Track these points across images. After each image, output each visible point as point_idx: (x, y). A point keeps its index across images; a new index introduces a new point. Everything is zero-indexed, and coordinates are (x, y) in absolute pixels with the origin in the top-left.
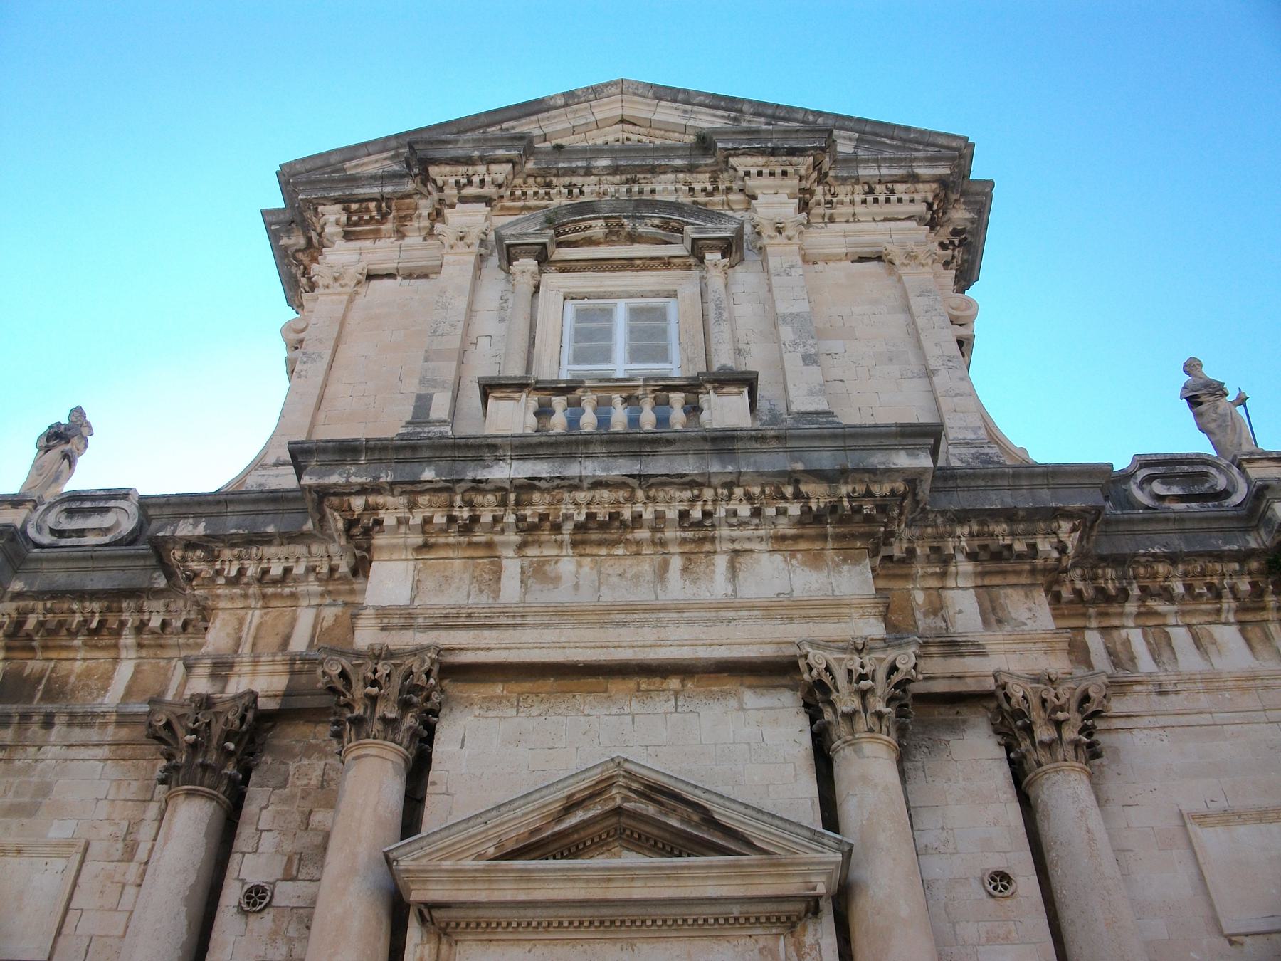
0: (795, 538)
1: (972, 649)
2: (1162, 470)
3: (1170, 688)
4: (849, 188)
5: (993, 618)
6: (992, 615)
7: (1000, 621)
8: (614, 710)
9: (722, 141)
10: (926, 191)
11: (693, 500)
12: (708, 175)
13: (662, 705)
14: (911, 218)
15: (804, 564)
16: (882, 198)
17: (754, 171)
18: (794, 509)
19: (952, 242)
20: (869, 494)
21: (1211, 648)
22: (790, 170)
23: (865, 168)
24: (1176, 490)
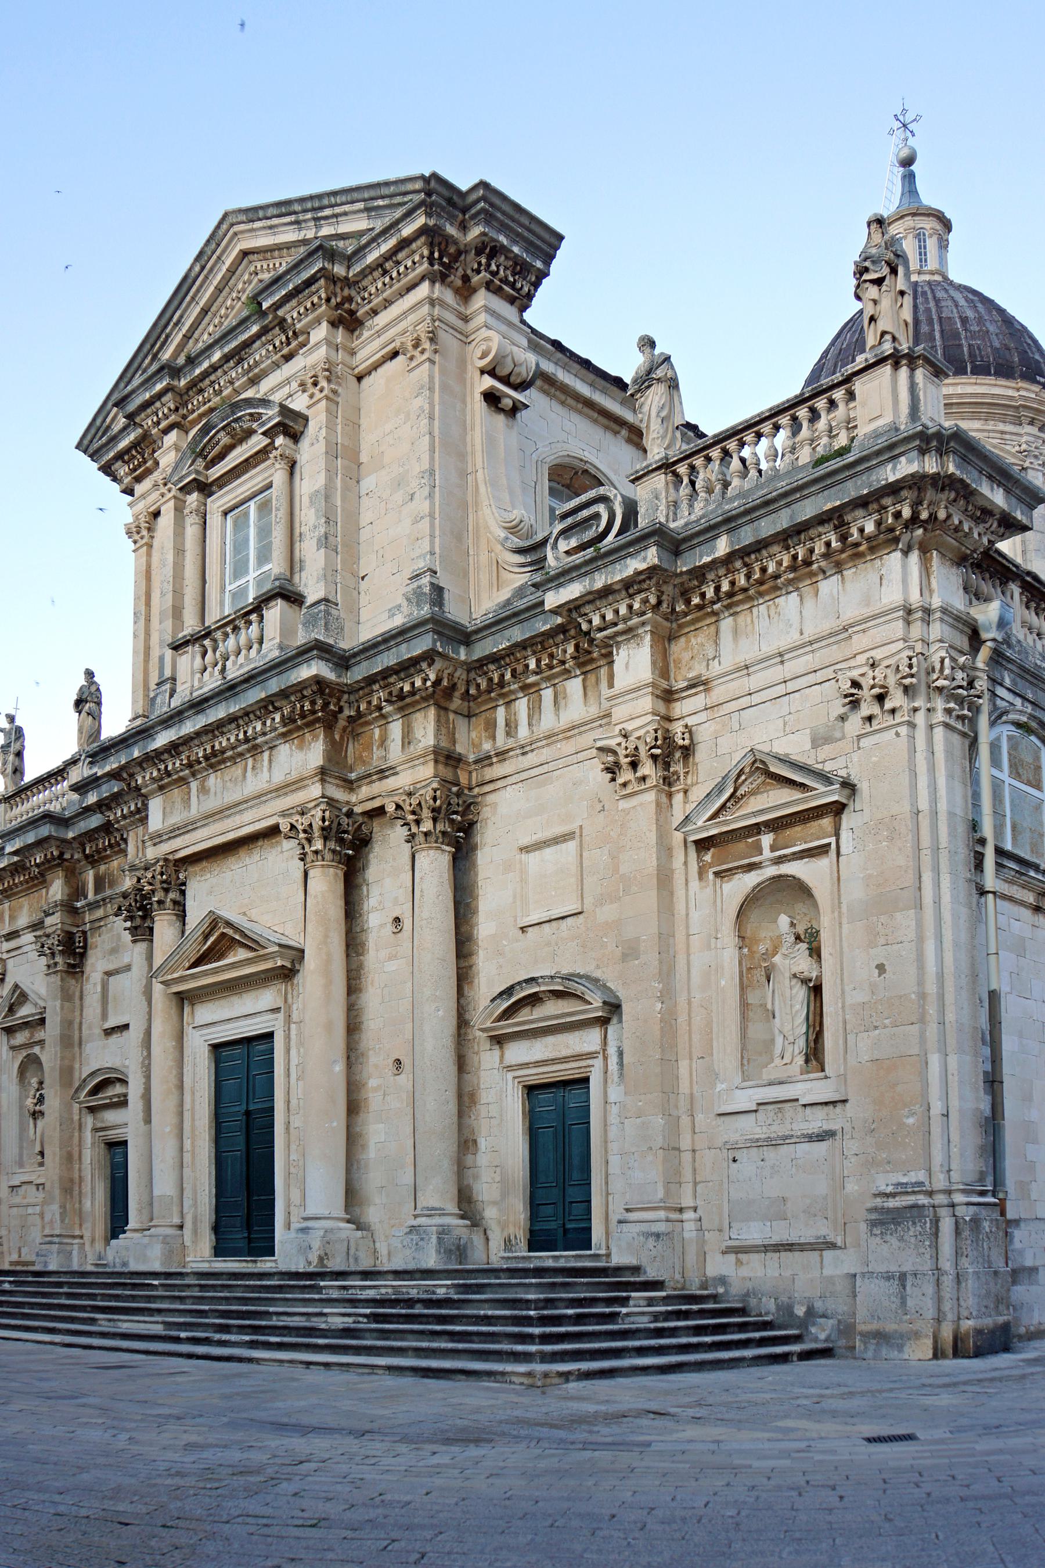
0: (290, 732)
1: (391, 772)
2: (569, 521)
3: (528, 748)
4: (370, 277)
5: (406, 740)
6: (407, 739)
7: (409, 743)
8: (241, 865)
9: (265, 299)
10: (421, 249)
11: (238, 726)
12: (277, 328)
13: (256, 855)
14: (423, 278)
15: (297, 748)
16: (394, 274)
17: (295, 315)
18: (278, 717)
19: (480, 264)
20: (304, 697)
21: (562, 703)
22: (316, 300)
23: (370, 252)
24: (573, 543)
